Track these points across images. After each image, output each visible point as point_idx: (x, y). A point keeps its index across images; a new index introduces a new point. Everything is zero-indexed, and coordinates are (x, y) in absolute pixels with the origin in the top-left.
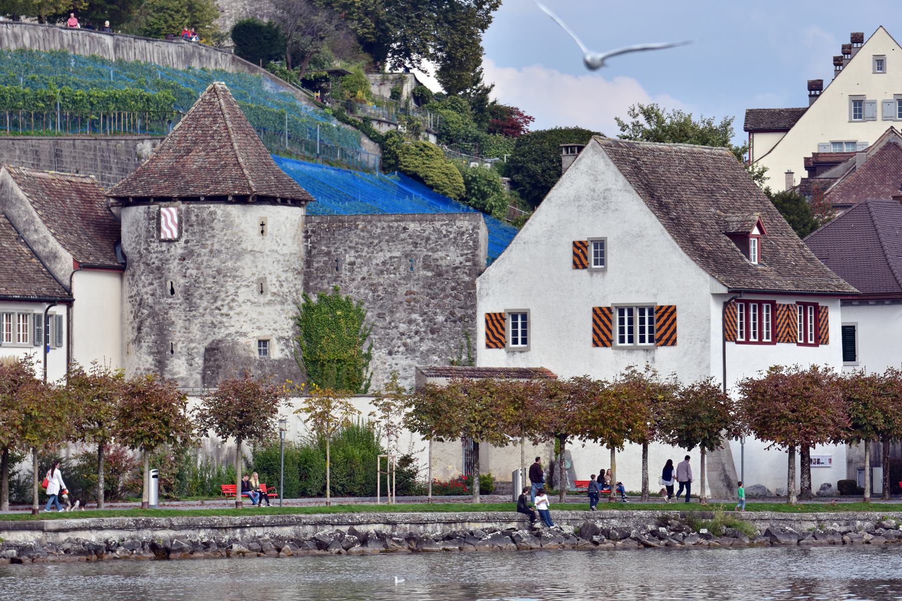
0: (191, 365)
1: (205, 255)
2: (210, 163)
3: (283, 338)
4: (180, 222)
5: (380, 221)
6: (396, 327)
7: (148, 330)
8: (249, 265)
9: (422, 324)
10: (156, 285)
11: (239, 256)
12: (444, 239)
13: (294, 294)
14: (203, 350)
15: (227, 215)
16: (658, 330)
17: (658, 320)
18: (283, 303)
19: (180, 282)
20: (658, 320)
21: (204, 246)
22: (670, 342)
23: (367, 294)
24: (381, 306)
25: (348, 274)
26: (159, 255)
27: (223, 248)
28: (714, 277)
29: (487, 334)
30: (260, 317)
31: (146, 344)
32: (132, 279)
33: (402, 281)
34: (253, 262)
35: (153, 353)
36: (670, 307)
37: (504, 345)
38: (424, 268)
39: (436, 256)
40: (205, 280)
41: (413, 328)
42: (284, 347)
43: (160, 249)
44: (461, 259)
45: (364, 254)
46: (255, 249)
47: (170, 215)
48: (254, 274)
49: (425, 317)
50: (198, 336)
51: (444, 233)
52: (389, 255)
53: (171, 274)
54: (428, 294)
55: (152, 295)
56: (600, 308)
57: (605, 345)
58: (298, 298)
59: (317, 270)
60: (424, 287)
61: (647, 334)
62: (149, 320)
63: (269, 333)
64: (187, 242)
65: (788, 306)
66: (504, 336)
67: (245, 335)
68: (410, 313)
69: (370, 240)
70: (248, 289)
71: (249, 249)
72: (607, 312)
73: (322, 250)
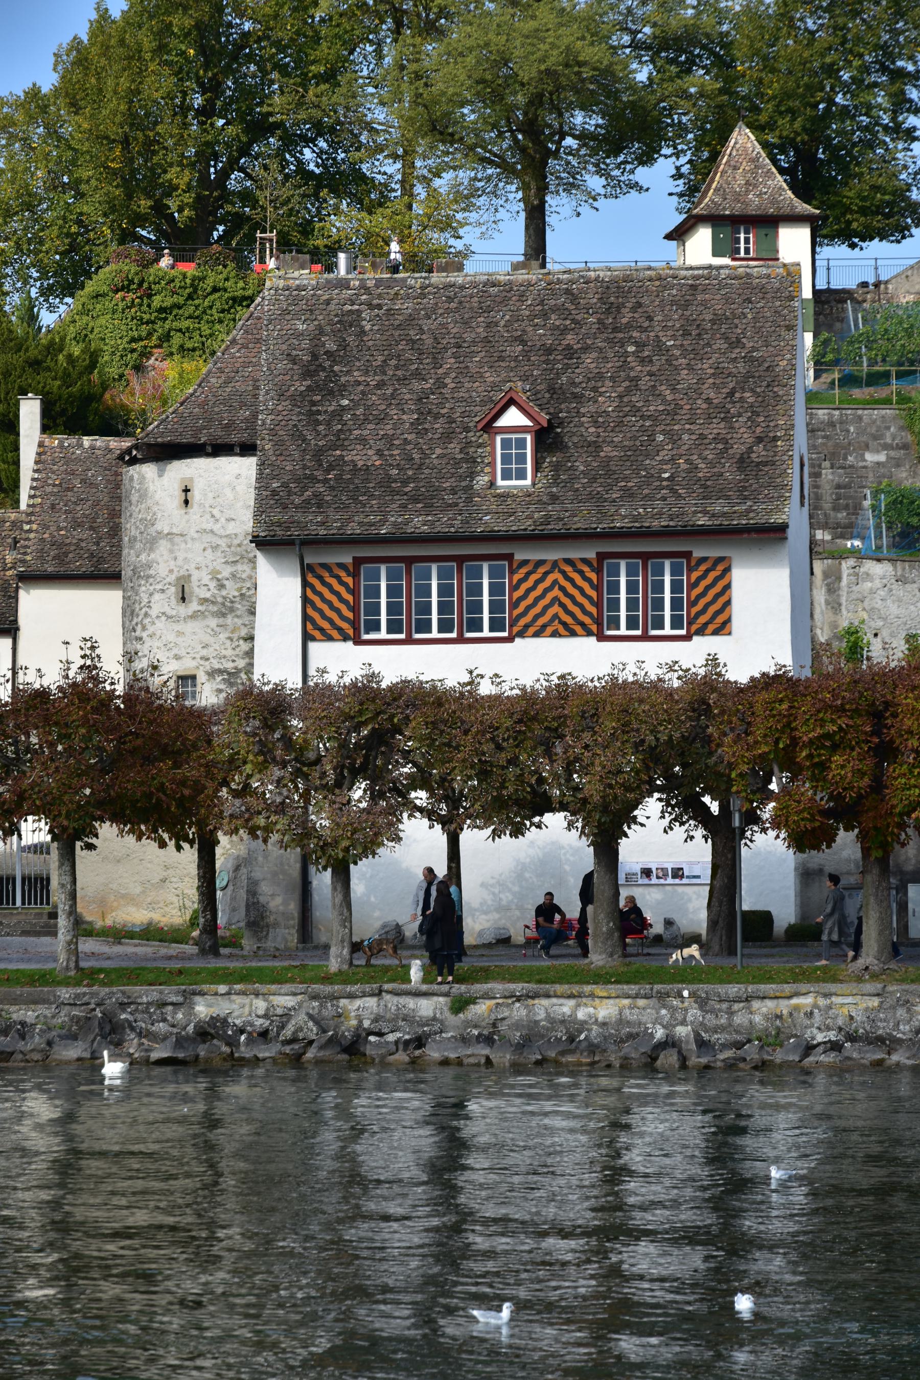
3: (220, 672)
11: (152, 543)
15: (143, 478)
30: (180, 640)
34: (171, 551)
46: (175, 531)
63: (194, 664)
65: (555, 564)
70: (162, 596)
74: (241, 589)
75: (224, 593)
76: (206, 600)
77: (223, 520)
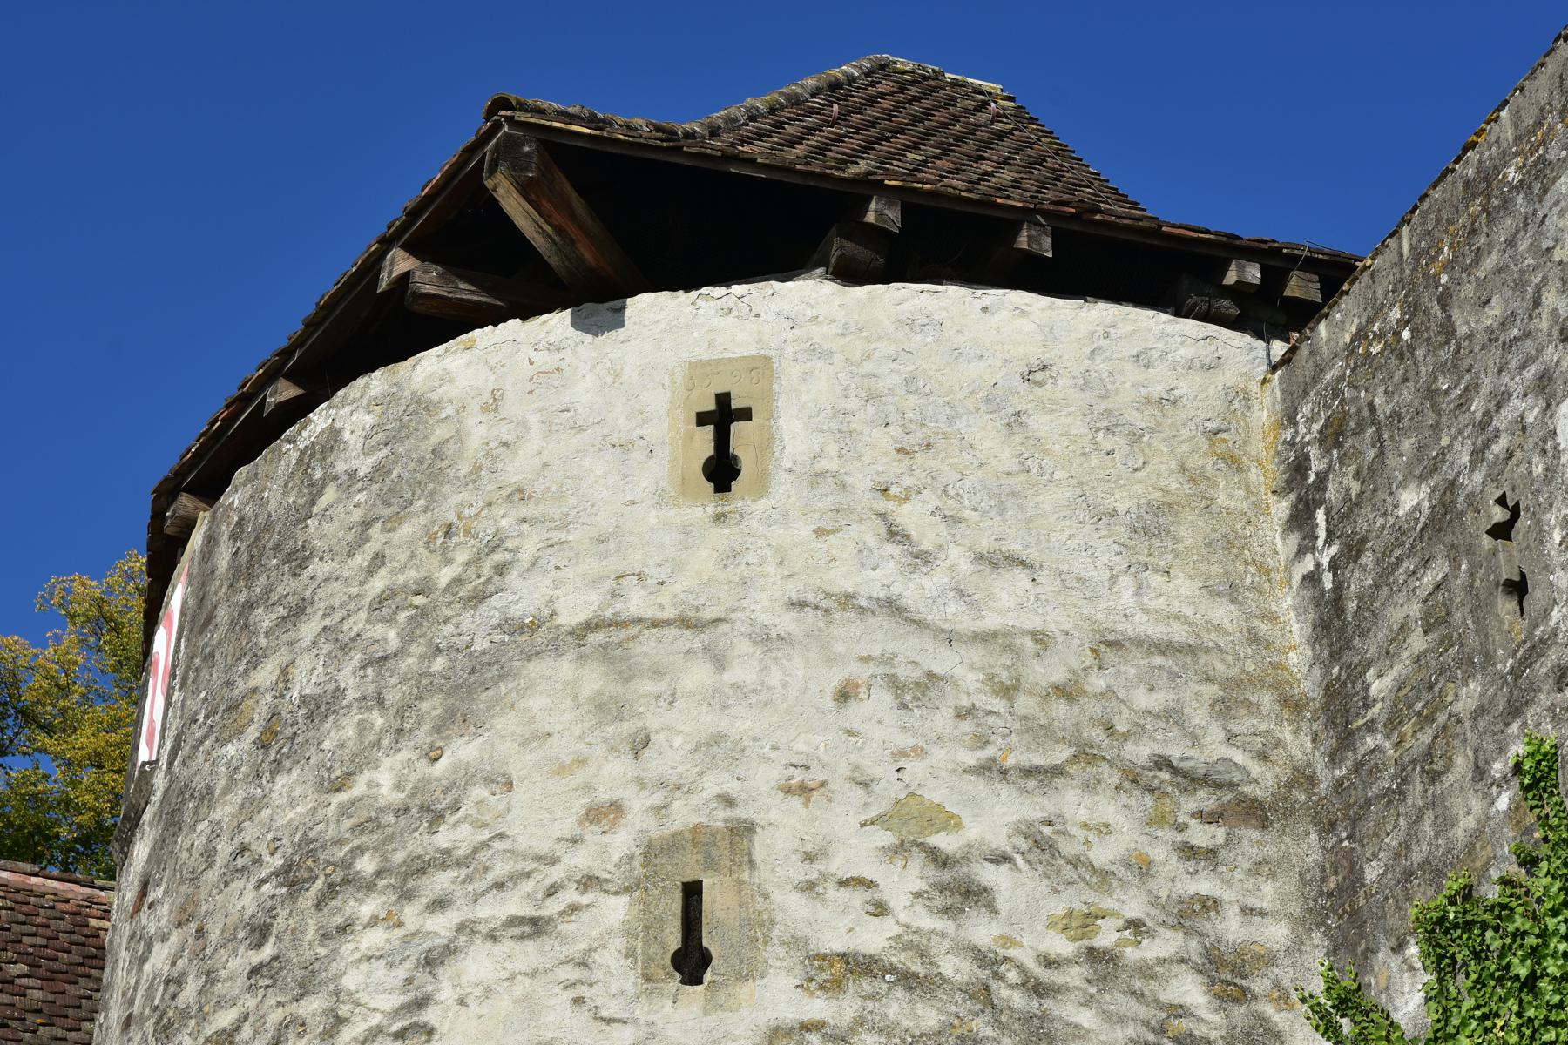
8: (563, 748)
11: (466, 691)
13: (1189, 990)
34: (606, 709)
46: (636, 603)
48: (604, 814)
70: (529, 954)
71: (572, 613)
74: (1082, 923)
75: (982, 931)
76: (857, 966)
77: (959, 557)
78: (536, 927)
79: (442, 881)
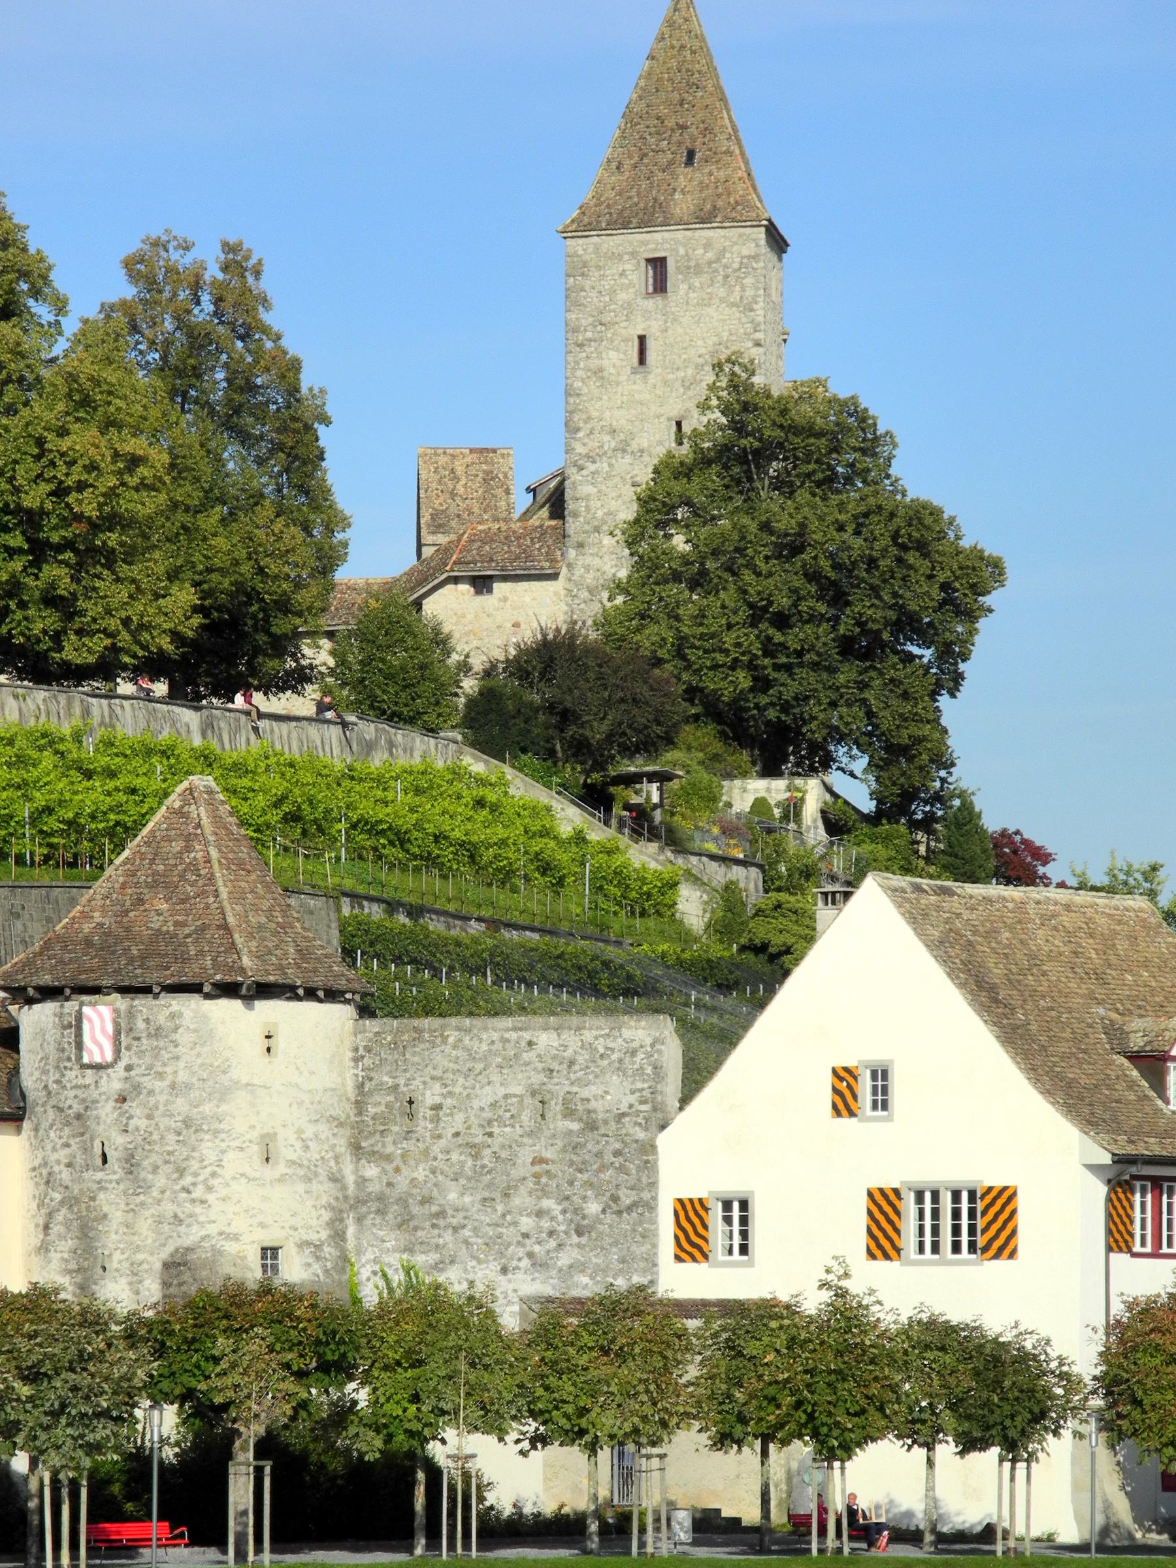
0: (137, 1293)
1: (161, 1092)
2: (176, 924)
3: (308, 1243)
4: (117, 1032)
5: (486, 1029)
6: (515, 1224)
7: (62, 1229)
9: (560, 1217)
10: (74, 1147)
11: (223, 1094)
12: (600, 1062)
13: (332, 1163)
14: (158, 1266)
15: (205, 1018)
16: (984, 1231)
17: (984, 1213)
18: (310, 1180)
19: (117, 1143)
20: (984, 1213)
21: (160, 1076)
22: (1007, 1252)
23: (462, 1164)
24: (489, 1186)
25: (430, 1126)
26: (79, 1092)
27: (194, 1080)
28: (1086, 1133)
29: (676, 1237)
31: (59, 1255)
32: (36, 1137)
33: (525, 1140)
35: (70, 1272)
36: (1005, 1188)
37: (706, 1257)
38: (565, 1116)
39: (585, 1093)
40: (162, 1138)
41: (546, 1224)
42: (310, 1260)
43: (80, 1081)
44: (633, 1099)
45: (457, 1090)
46: (255, 1081)
47: (99, 1017)
49: (566, 1204)
50: (150, 1241)
51: (602, 1051)
52: (502, 1091)
53: (102, 1127)
54: (572, 1163)
55: (69, 1165)
56: (881, 1190)
57: (887, 1257)
58: (340, 1170)
59: (373, 1119)
60: (564, 1150)
61: (965, 1238)
62: (64, 1211)
63: (283, 1233)
64: (129, 1068)
66: (706, 1240)
67: (236, 1237)
68: (539, 1198)
69: (469, 1065)
71: (244, 1082)
72: (892, 1197)
73: (382, 1084)
76: (294, 1162)
78: (242, 1149)
79: (223, 1136)
